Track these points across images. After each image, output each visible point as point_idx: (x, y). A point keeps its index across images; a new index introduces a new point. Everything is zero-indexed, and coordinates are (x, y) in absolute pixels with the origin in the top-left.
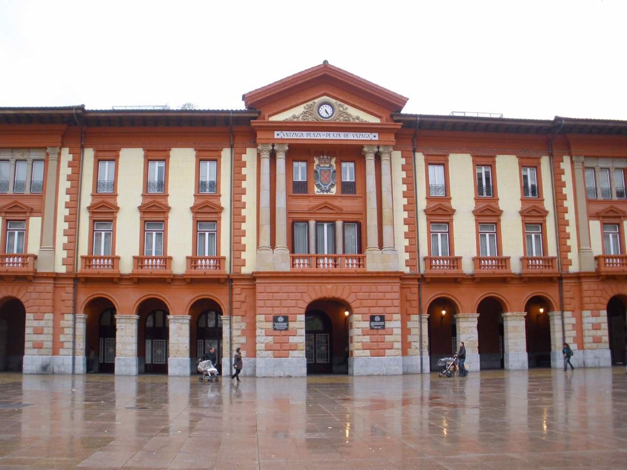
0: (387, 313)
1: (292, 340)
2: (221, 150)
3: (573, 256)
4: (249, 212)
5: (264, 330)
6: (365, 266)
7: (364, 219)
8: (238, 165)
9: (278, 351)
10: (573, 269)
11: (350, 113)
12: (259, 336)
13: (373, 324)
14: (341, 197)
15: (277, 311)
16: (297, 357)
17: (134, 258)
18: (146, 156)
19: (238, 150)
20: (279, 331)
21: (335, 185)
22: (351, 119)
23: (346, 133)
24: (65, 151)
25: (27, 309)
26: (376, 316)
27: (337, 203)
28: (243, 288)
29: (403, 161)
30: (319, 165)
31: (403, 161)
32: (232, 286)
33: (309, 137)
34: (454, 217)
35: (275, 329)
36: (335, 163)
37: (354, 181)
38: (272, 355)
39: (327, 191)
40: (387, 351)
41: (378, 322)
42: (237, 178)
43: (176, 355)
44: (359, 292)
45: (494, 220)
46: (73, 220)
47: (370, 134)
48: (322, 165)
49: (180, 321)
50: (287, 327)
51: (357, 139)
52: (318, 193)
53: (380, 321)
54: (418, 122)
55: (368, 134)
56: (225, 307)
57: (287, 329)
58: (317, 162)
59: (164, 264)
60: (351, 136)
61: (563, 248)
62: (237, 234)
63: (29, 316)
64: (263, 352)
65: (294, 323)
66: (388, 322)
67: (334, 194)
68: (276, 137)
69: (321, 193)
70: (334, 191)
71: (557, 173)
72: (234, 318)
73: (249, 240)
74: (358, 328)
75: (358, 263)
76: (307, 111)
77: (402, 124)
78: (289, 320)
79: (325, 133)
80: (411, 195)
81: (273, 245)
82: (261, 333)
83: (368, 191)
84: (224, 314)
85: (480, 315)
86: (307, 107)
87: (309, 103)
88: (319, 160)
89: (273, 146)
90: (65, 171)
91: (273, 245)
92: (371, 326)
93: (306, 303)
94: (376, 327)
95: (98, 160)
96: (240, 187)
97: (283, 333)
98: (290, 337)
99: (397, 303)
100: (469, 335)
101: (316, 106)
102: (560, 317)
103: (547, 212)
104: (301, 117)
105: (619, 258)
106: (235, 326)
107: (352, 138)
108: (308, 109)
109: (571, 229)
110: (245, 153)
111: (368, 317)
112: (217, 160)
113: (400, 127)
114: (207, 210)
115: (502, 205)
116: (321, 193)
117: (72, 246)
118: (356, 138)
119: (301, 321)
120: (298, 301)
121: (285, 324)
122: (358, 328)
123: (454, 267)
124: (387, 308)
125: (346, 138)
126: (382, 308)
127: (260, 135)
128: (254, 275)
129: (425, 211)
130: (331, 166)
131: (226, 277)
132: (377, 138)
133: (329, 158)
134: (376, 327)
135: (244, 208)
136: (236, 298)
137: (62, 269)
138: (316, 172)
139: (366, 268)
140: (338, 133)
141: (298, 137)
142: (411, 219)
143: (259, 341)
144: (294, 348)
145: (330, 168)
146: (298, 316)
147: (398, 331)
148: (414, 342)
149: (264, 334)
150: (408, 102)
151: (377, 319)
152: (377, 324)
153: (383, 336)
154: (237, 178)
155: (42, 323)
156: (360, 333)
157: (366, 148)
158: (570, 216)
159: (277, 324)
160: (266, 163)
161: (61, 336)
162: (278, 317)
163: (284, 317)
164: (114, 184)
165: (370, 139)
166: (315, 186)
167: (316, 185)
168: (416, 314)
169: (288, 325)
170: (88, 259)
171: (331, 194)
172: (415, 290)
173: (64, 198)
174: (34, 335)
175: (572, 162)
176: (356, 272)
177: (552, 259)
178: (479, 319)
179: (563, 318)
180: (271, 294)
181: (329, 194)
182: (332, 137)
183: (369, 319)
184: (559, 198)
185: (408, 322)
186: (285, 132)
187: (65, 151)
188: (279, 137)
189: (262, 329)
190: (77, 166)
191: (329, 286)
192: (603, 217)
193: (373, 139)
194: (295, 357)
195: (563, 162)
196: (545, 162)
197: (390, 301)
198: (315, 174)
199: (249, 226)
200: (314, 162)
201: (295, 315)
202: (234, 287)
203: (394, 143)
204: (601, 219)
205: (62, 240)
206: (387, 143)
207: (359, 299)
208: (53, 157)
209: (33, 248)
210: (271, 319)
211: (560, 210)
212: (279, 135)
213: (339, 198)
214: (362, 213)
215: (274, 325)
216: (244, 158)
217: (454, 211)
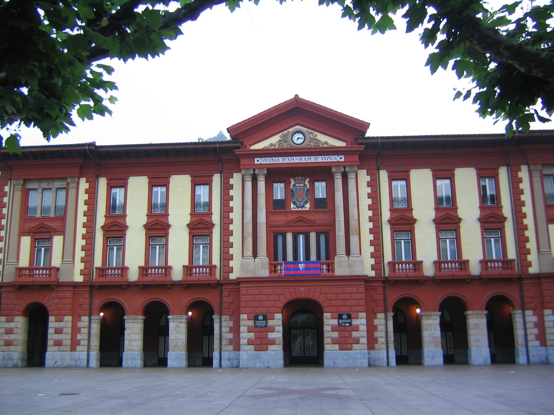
1: (271, 335)
3: (532, 257)
4: (236, 227)
5: (246, 328)
6: (333, 271)
8: (226, 187)
9: (259, 345)
10: (533, 270)
11: (319, 139)
12: (242, 332)
15: (258, 310)
16: (276, 351)
17: (140, 267)
18: (192, 181)
22: (320, 144)
23: (316, 157)
24: (83, 180)
25: (50, 313)
26: (344, 314)
27: (310, 217)
28: (230, 292)
29: (368, 178)
30: (294, 185)
31: (368, 178)
32: (221, 289)
33: (284, 162)
34: (416, 225)
35: (256, 326)
36: (309, 182)
37: (326, 197)
38: (253, 349)
39: (302, 207)
40: (354, 345)
41: (345, 319)
42: (226, 198)
43: (175, 349)
45: (498, 226)
46: (89, 237)
47: (337, 156)
48: (297, 185)
49: (178, 320)
50: (266, 324)
51: (325, 161)
52: (294, 209)
53: (348, 319)
55: (335, 156)
56: (216, 308)
57: (266, 326)
58: (293, 182)
59: (50, 273)
60: (320, 159)
61: (523, 251)
62: (226, 245)
63: (52, 319)
64: (246, 346)
67: (308, 209)
68: (256, 162)
69: (297, 209)
70: (308, 206)
71: (515, 182)
72: (224, 317)
73: (235, 251)
74: (328, 325)
76: (282, 140)
77: (364, 146)
79: (298, 158)
80: (375, 207)
81: (255, 255)
82: (244, 329)
84: (215, 314)
85: (441, 314)
87: (284, 133)
88: (295, 180)
90: (83, 197)
91: (255, 255)
92: (339, 324)
93: (283, 303)
94: (343, 324)
95: (110, 187)
97: (263, 329)
98: (269, 334)
99: (362, 302)
100: (433, 332)
101: (290, 135)
102: (521, 315)
103: (505, 219)
104: (277, 144)
105: (501, 261)
106: (224, 324)
107: (322, 161)
109: (530, 233)
110: (232, 178)
111: (336, 315)
112: (209, 183)
114: (200, 226)
115: (461, 213)
116: (297, 209)
117: (88, 259)
118: (324, 161)
119: (279, 319)
121: (265, 321)
122: (328, 325)
123: (103, 276)
127: (243, 162)
128: (238, 280)
129: (389, 221)
130: (305, 185)
131: (216, 282)
132: (343, 160)
133: (303, 178)
134: (343, 324)
136: (225, 299)
137: (79, 278)
138: (292, 191)
140: (309, 157)
141: (275, 162)
143: (243, 337)
144: (273, 342)
145: (305, 187)
146: (276, 315)
147: (363, 328)
148: (380, 337)
149: (246, 330)
151: (345, 316)
152: (344, 321)
153: (350, 332)
154: (226, 198)
155: (62, 324)
156: (330, 330)
158: (529, 221)
160: (249, 185)
161: (78, 335)
162: (258, 316)
163: (263, 316)
164: (166, 206)
166: (292, 203)
167: (292, 202)
168: (381, 312)
169: (266, 323)
170: (102, 271)
171: (306, 209)
172: (380, 291)
173: (82, 219)
174: (6, 335)
175: (530, 172)
176: (325, 276)
177: (512, 261)
178: (487, 315)
179: (524, 316)
181: (304, 209)
182: (304, 161)
184: (517, 204)
185: (374, 320)
186: (263, 159)
187: (83, 180)
188: (259, 163)
189: (245, 326)
190: (92, 192)
191: (302, 289)
192: (34, 233)
193: (340, 160)
194: (273, 351)
195: (520, 171)
196: (503, 173)
199: (236, 239)
200: (290, 183)
202: (223, 290)
203: (358, 163)
204: (32, 234)
205: (80, 254)
208: (73, 185)
209: (56, 262)
211: (519, 216)
212: (259, 161)
213: (312, 213)
214: (332, 225)
215: (255, 323)
216: (232, 181)
217: (415, 220)
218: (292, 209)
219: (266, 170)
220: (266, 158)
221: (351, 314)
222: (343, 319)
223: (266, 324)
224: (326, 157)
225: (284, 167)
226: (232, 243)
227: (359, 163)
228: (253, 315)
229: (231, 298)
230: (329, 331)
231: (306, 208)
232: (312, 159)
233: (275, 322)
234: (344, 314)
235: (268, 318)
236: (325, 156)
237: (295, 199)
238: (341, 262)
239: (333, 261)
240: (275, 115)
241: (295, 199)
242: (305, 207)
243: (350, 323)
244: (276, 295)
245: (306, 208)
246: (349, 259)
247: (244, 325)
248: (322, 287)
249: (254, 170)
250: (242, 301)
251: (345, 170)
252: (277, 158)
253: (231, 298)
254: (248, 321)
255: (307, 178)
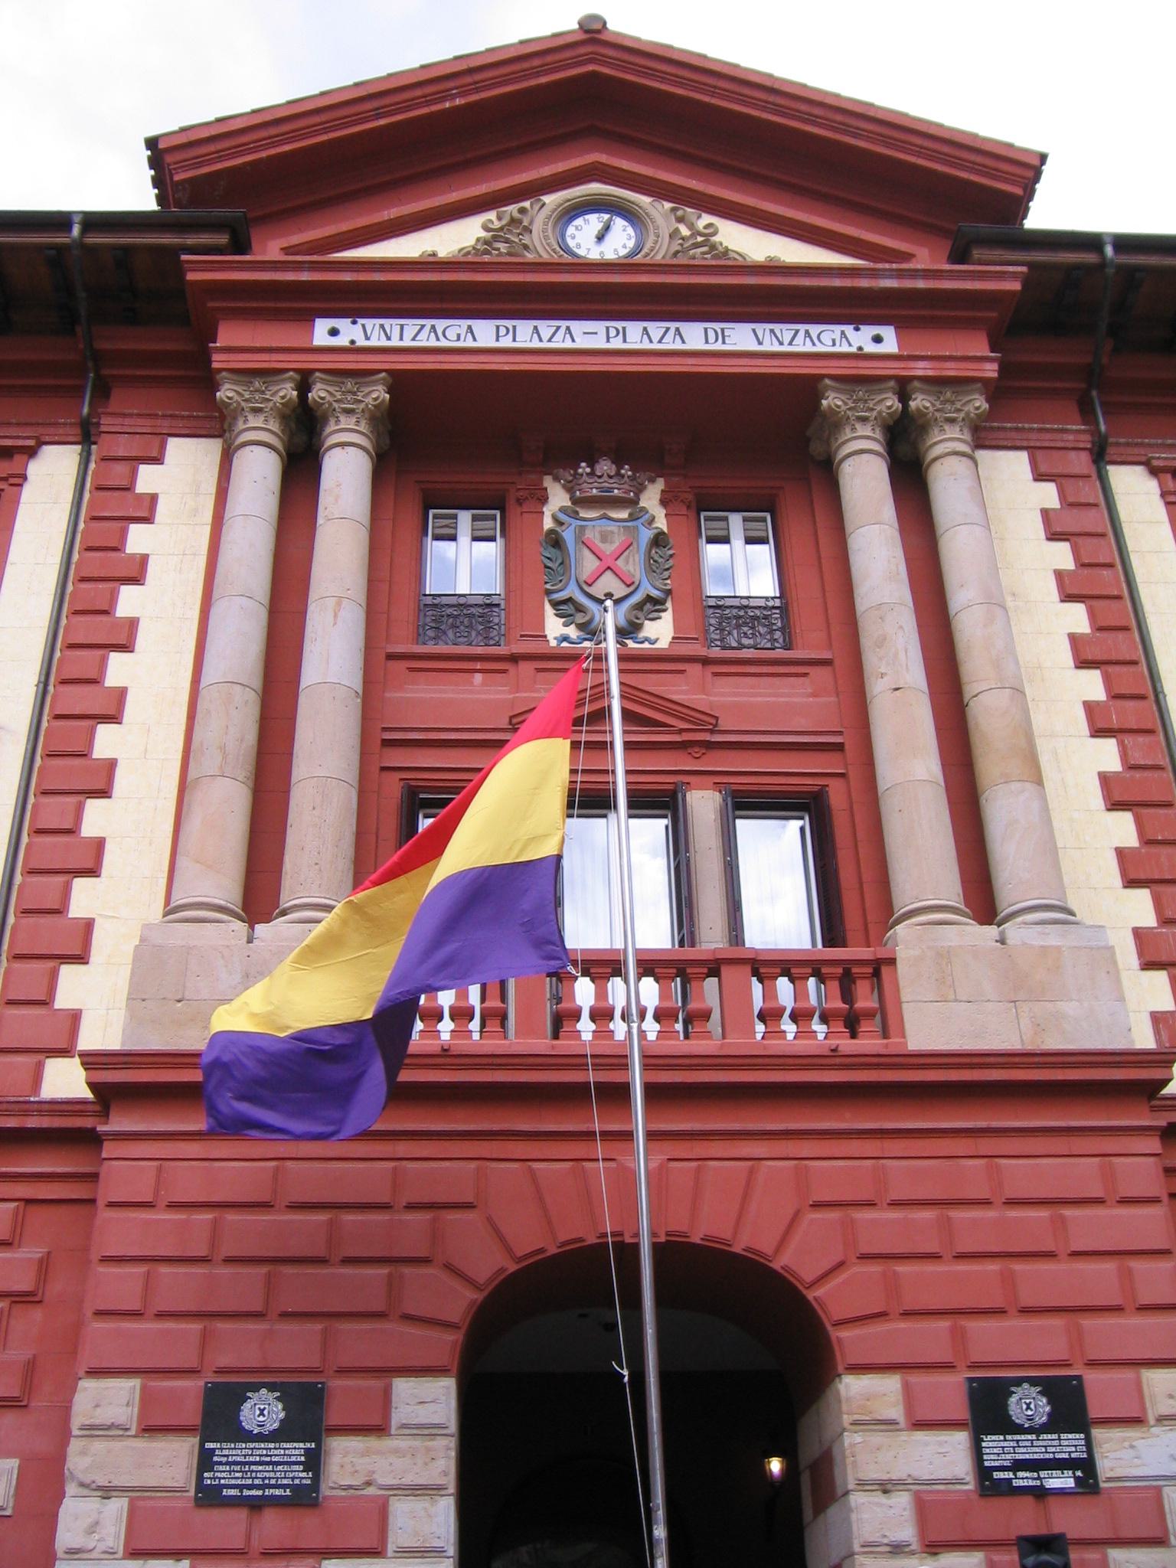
0: (1092, 1364)
2: (32, 452)
5: (119, 1506)
7: (854, 774)
12: (73, 1553)
13: (998, 1448)
14: (706, 661)
19: (122, 447)
20: (240, 1516)
21: (669, 604)
23: (717, 326)
27: (683, 689)
28: (29, 1201)
31: (1048, 495)
33: (506, 342)
35: (209, 1496)
36: (664, 502)
44: (870, 1204)
47: (849, 329)
50: (305, 1477)
51: (776, 348)
54: (1110, 271)
57: (305, 1498)
58: (558, 498)
65: (372, 1442)
66: (1116, 1434)
67: (664, 643)
74: (886, 1487)
75: (838, 1004)
77: (1024, 269)
78: (333, 1418)
79: (599, 326)
82: (92, 1528)
83: (862, 604)
86: (497, 224)
87: (512, 209)
89: (304, 387)
92: (983, 1473)
94: (1024, 1479)
96: (105, 612)
97: (273, 1527)
107: (752, 346)
108: (501, 229)
110: (158, 460)
113: (1016, 286)
118: (770, 346)
119: (428, 1430)
120: (407, 1271)
121: (296, 1450)
122: (886, 1487)
124: (1088, 1322)
125: (719, 346)
126: (1057, 1322)
127: (228, 335)
134: (1024, 1479)
135: (114, 718)
138: (555, 541)
139: (902, 1034)
142: (1138, 775)
146: (404, 1388)
150: (1046, 169)
152: (1031, 1448)
156: (907, 1532)
157: (831, 395)
159: (225, 1451)
165: (854, 350)
166: (549, 611)
167: (555, 604)
169: (314, 1462)
171: (646, 645)
180: (207, 1216)
183: (963, 1412)
186: (370, 323)
188: (341, 341)
189: (107, 1492)
193: (871, 348)
197: (1109, 1266)
198: (551, 552)
200: (544, 499)
201: (374, 1383)
203: (991, 370)
206: (951, 370)
207: (865, 1257)
210: (192, 1413)
213: (695, 670)
214: (839, 747)
215: (206, 1461)
218: (553, 643)
219: (381, 388)
220: (387, 322)
221: (1079, 1378)
222: (1019, 1429)
223: (305, 1477)
224: (785, 331)
225: (506, 367)
226: (99, 846)
227: (995, 366)
228: (193, 1386)
229: (30, 1252)
230: (897, 1549)
231: (647, 639)
232: (695, 336)
233: (396, 1451)
234: (1018, 1382)
235: (334, 1415)
236: (777, 327)
237: (573, 582)
238: (944, 956)
239: (882, 953)
240: (458, 102)
241: (573, 582)
242: (642, 635)
243: (1085, 1467)
244: (411, 1207)
245: (653, 642)
246: (1002, 941)
247: (102, 1481)
248: (806, 1148)
249: (304, 387)
250: (106, 1260)
251: (905, 405)
252: (465, 323)
253: (30, 1252)
254: (141, 1444)
255: (652, 481)
